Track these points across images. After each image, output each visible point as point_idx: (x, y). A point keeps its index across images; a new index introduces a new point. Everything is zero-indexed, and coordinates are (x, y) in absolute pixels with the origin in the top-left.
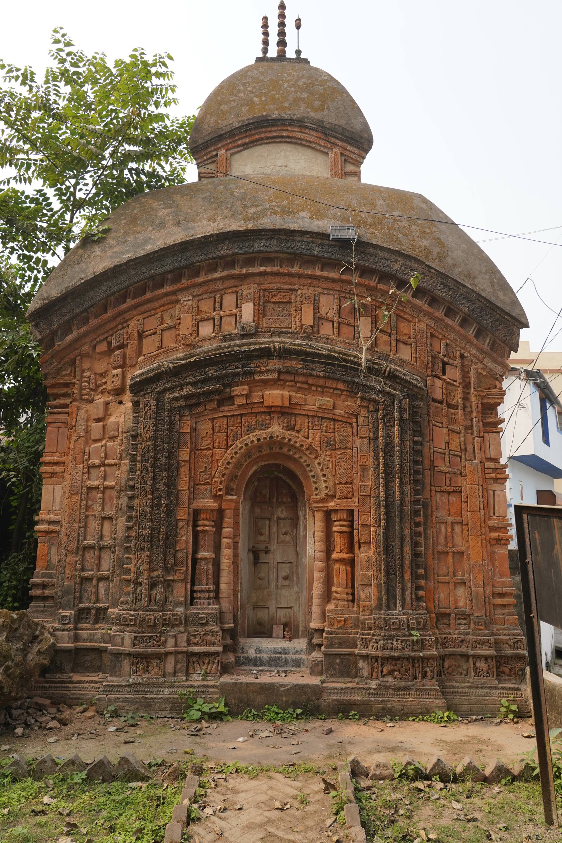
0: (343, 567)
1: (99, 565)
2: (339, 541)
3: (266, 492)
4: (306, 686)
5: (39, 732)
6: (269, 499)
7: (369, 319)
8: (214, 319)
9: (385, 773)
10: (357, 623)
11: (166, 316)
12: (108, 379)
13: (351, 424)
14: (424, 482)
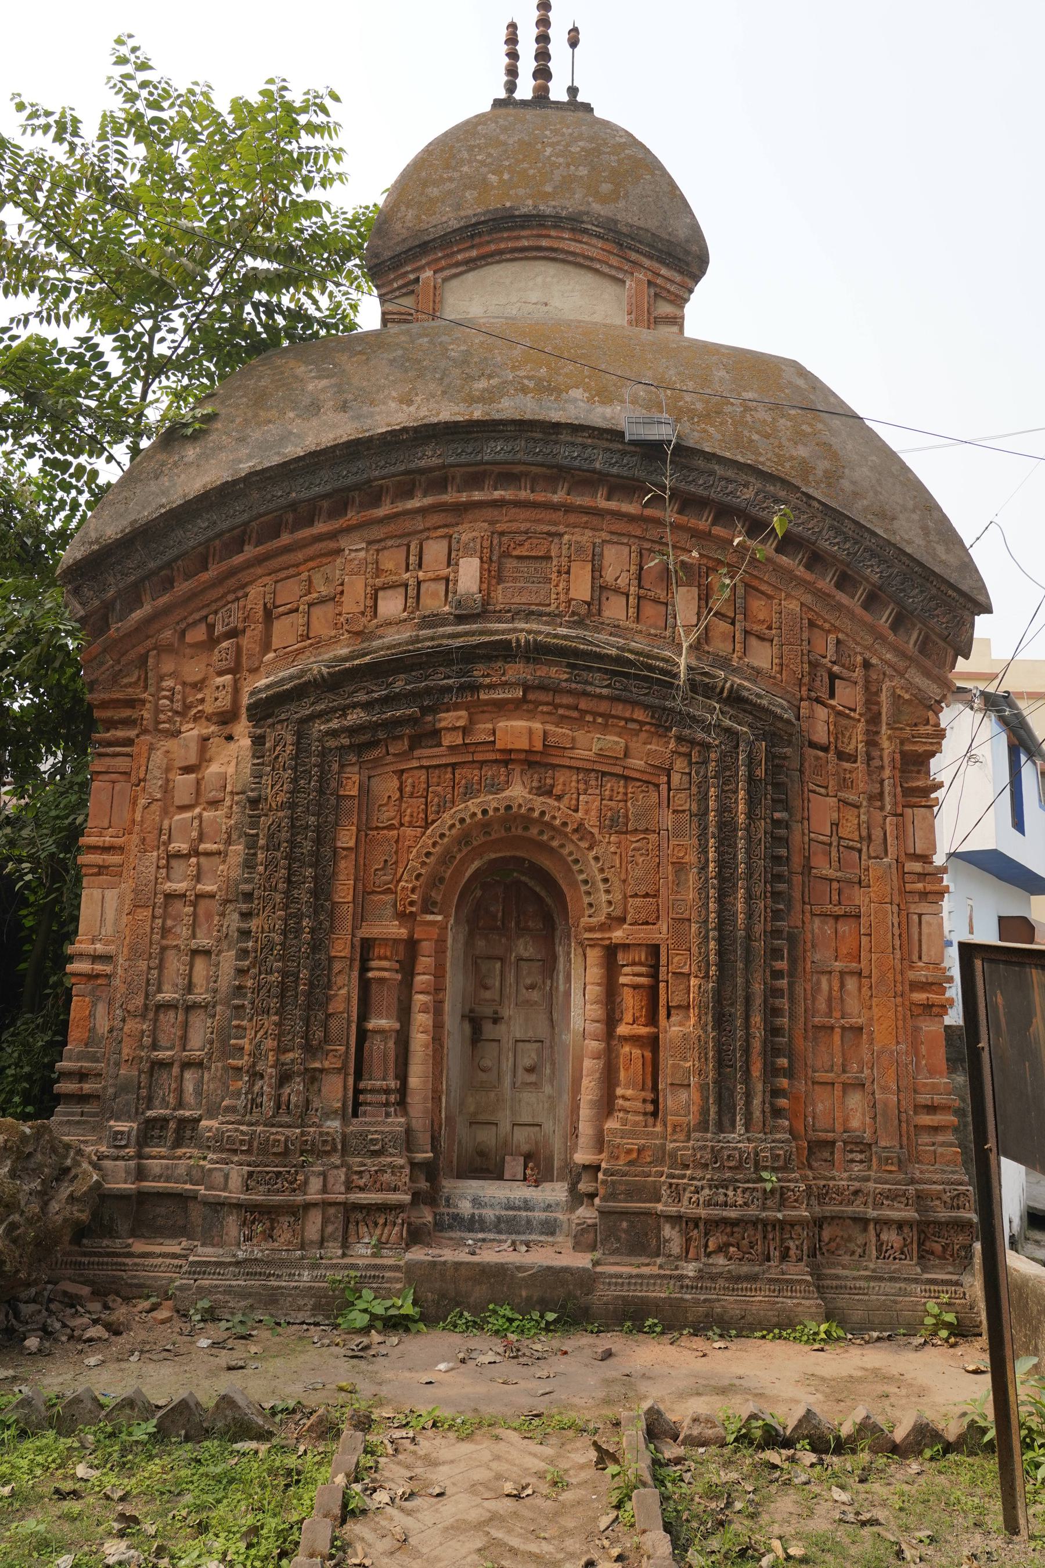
0: (637, 1052)
1: (184, 1038)
3: (497, 909)
4: (566, 1270)
5: (69, 1346)
6: (503, 923)
8: (406, 586)
9: (710, 1433)
10: (661, 1156)
11: (318, 579)
12: (208, 693)
13: (657, 786)
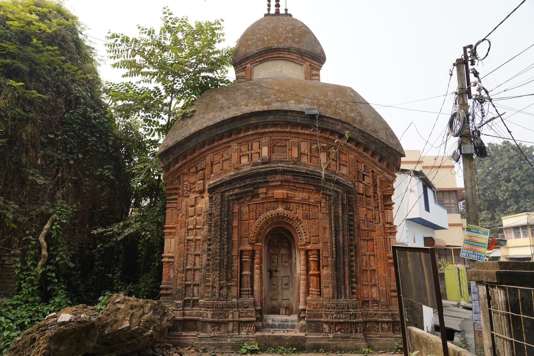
0: (315, 278)
1: (194, 278)
2: (312, 265)
4: (298, 337)
7: (326, 153)
11: (225, 154)
12: (196, 185)
14: (355, 235)
